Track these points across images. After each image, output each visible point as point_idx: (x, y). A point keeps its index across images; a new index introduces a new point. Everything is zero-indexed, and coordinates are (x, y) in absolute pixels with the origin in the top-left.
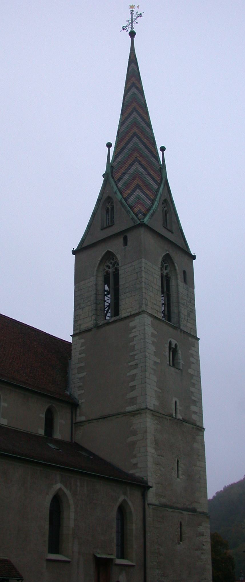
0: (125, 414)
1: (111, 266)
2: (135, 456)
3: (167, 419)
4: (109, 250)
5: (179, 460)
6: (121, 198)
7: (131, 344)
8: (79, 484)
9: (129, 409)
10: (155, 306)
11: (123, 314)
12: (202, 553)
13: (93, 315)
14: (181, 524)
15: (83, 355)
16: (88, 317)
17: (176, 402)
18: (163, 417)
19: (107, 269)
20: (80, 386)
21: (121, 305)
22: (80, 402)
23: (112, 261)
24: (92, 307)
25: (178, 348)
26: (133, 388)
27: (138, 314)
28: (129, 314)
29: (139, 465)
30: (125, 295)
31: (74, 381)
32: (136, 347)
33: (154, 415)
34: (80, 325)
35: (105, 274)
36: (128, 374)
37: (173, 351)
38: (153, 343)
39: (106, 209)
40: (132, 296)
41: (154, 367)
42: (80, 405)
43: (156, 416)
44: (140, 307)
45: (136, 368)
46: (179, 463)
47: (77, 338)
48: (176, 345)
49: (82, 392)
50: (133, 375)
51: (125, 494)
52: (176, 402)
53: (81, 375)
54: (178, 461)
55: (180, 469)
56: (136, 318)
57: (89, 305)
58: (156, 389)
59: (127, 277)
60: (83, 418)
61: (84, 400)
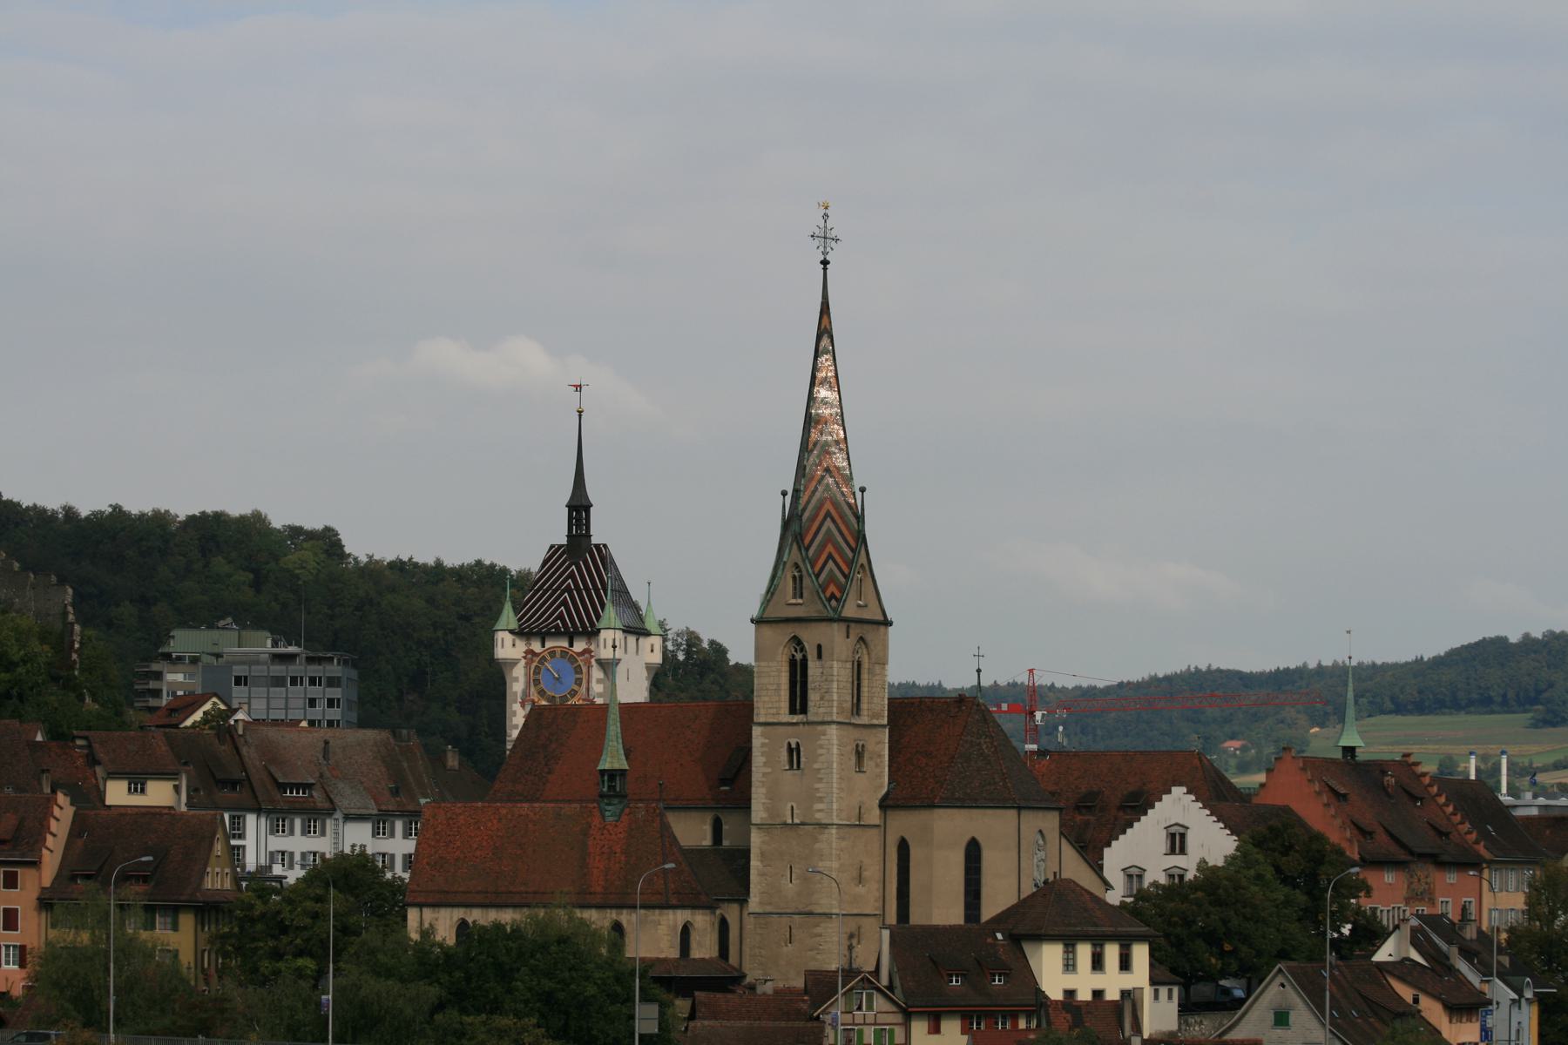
14: (790, 927)
17: (792, 807)
37: (794, 752)
41: (764, 779)
48: (798, 744)
52: (792, 807)
54: (791, 867)
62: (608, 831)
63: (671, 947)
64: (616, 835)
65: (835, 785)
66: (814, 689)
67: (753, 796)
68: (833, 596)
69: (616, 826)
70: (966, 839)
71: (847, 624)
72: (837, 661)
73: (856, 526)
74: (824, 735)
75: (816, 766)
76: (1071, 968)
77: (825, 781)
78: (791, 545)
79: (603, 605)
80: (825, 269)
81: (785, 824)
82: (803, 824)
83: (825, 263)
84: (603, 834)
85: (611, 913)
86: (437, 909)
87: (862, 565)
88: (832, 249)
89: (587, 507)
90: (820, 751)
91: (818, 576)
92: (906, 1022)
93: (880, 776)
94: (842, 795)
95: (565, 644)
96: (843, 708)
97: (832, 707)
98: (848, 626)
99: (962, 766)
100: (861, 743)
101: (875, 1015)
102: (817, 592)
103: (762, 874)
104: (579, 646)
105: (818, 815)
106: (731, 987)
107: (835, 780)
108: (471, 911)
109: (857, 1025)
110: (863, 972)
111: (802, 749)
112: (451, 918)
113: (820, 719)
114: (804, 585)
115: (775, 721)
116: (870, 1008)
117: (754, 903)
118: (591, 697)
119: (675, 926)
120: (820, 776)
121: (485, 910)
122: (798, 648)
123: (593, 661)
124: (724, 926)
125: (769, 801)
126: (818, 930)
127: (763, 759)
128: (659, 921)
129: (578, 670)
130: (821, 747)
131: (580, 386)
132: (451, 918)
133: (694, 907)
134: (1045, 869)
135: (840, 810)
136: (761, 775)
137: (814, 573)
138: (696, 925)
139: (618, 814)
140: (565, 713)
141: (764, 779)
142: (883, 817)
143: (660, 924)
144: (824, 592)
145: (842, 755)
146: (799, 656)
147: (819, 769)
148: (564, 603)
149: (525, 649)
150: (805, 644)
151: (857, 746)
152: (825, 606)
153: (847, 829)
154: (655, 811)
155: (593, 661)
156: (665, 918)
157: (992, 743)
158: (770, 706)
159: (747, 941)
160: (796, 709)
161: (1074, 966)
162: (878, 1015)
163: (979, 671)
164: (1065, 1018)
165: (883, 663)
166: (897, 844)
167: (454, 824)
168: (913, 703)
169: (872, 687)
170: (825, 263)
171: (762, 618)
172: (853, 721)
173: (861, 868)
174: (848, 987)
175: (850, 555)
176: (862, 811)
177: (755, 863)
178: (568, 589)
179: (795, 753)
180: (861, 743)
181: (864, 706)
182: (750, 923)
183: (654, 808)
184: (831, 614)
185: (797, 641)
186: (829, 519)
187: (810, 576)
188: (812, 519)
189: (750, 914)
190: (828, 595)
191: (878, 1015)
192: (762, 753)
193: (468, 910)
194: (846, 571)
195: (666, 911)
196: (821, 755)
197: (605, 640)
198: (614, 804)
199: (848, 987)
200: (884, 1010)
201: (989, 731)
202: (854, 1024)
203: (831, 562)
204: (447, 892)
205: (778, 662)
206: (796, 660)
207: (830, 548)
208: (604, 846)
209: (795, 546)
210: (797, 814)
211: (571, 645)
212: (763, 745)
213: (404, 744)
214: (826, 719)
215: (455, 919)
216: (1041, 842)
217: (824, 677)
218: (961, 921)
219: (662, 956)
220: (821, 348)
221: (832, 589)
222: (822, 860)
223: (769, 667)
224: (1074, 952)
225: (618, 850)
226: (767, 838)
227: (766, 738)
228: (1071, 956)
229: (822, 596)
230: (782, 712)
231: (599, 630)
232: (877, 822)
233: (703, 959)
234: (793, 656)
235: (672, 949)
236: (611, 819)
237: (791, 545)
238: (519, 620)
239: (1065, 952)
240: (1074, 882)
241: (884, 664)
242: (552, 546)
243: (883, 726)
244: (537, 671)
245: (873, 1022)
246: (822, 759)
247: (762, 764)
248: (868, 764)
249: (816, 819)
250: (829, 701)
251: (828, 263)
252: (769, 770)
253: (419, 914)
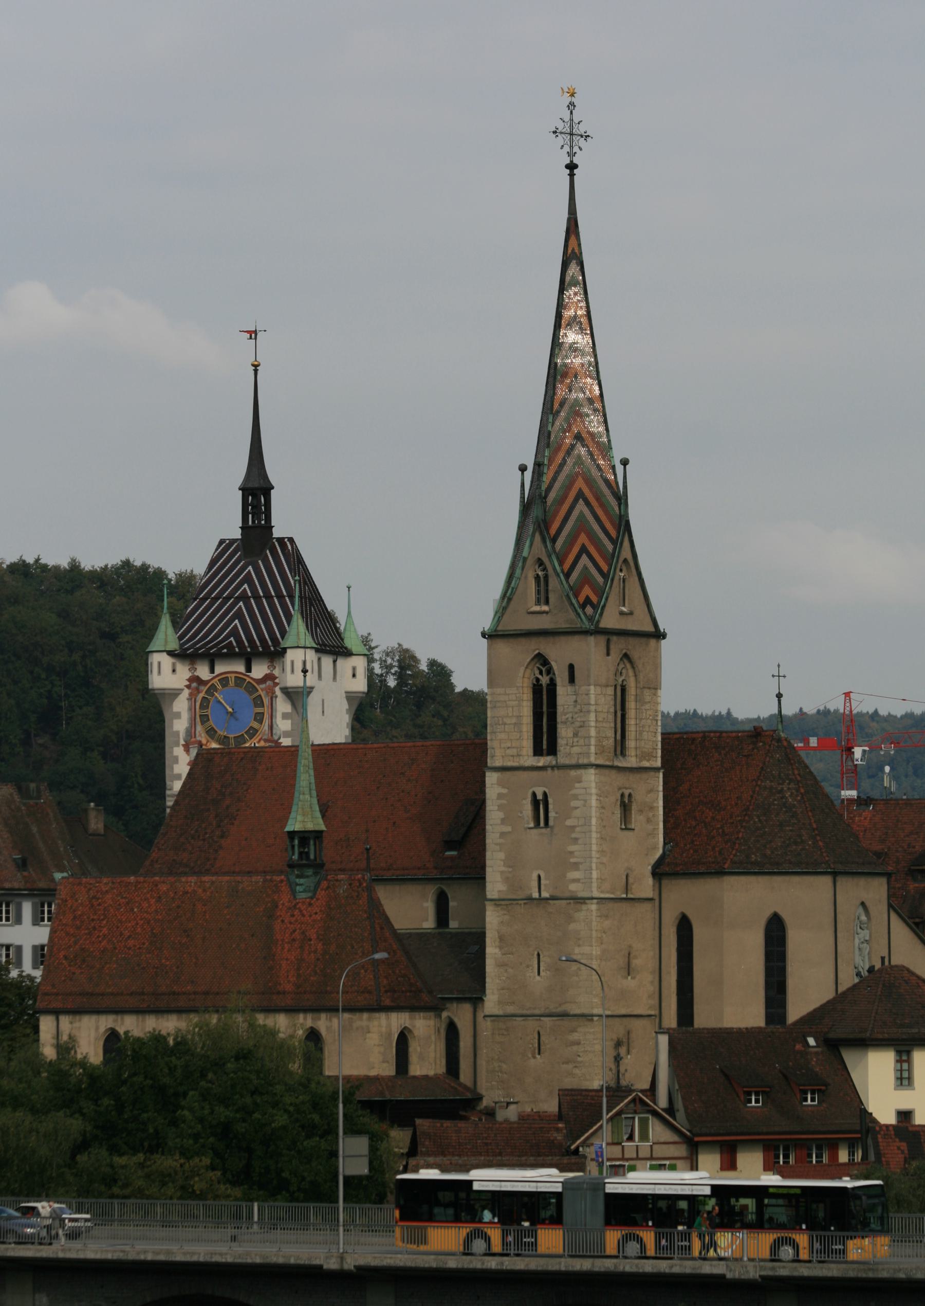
3: (521, 904)
5: (540, 953)
12: (576, 1067)
17: (539, 877)
18: (512, 904)
37: (540, 805)
38: (500, 808)
41: (501, 841)
43: (501, 905)
46: (541, 957)
48: (545, 794)
52: (539, 877)
54: (539, 955)
55: (542, 964)
58: (503, 869)
62: (301, 911)
63: (383, 1062)
64: (310, 916)
65: (594, 847)
66: (565, 723)
67: (488, 863)
68: (588, 601)
69: (310, 904)
70: (767, 914)
71: (607, 637)
72: (595, 685)
73: (617, 509)
74: (580, 782)
75: (569, 823)
76: (905, 1082)
77: (580, 842)
78: (533, 536)
79: (289, 617)
80: (572, 175)
81: (530, 899)
82: (553, 898)
83: (572, 167)
84: (293, 916)
85: (305, 1019)
86: (78, 1017)
87: (625, 561)
88: (580, 149)
89: (267, 489)
90: (574, 803)
91: (568, 575)
92: (692, 1154)
93: (653, 834)
94: (605, 860)
95: (241, 668)
96: (603, 747)
97: (589, 745)
98: (608, 641)
99: (760, 820)
100: (627, 792)
101: (651, 1146)
102: (568, 596)
103: (501, 965)
104: (259, 670)
105: (573, 887)
106: (462, 1113)
107: (594, 841)
108: (122, 1019)
109: (627, 1160)
110: (634, 1091)
111: (550, 800)
112: (97, 1028)
113: (574, 762)
114: (550, 588)
115: (515, 764)
116: (644, 1137)
117: (492, 1002)
118: (276, 738)
119: (390, 1034)
120: (573, 835)
121: (140, 1017)
122: (544, 669)
123: (277, 689)
124: (452, 1032)
125: (510, 870)
126: (575, 1036)
127: (501, 815)
128: (368, 1027)
129: (258, 702)
130: (576, 797)
131: (255, 332)
132: (97, 1028)
133: (413, 1008)
134: (869, 953)
135: (601, 880)
136: (498, 835)
137: (563, 571)
138: (416, 1033)
139: (312, 888)
140: (242, 759)
141: (501, 841)
142: (657, 885)
143: (369, 1032)
144: (576, 596)
145: (603, 808)
146: (544, 680)
147: (574, 827)
148: (239, 615)
149: (188, 675)
150: (553, 664)
151: (622, 795)
152: (578, 614)
153: (611, 905)
154: (361, 884)
155: (277, 689)
156: (376, 1023)
157: (798, 790)
158: (509, 745)
159: (483, 1052)
160: (542, 749)
161: (910, 1079)
162: (655, 1147)
163: (779, 696)
164: (899, 1148)
165: (654, 686)
166: (677, 922)
167: (99, 905)
168: (694, 739)
169: (641, 719)
170: (572, 167)
171: (496, 631)
172: (617, 763)
173: (629, 954)
174: (614, 1111)
175: (610, 547)
176: (631, 880)
177: (492, 950)
178: (244, 597)
179: (541, 806)
180: (627, 792)
181: (631, 744)
182: (486, 1027)
183: (359, 880)
184: (587, 625)
185: (542, 661)
186: (581, 501)
187: (558, 575)
188: (561, 501)
189: (485, 1016)
190: (582, 599)
191: (655, 1147)
192: (498, 806)
193: (119, 1017)
194: (605, 568)
195: (377, 1015)
196: (576, 808)
197: (292, 662)
198: (307, 877)
199: (614, 1111)
200: (662, 1140)
201: (794, 774)
202: (623, 1159)
203: (584, 557)
204: (92, 994)
205: (518, 687)
206: (541, 685)
207: (583, 539)
208: (294, 931)
209: (538, 537)
210: (545, 885)
211: (249, 669)
212: (500, 796)
213: (32, 802)
214: (581, 762)
215: (102, 1029)
216: (864, 918)
217: (578, 707)
218: (760, 1022)
219: (373, 1073)
220: (568, 279)
221: (587, 591)
222: (579, 946)
223: (505, 694)
224: (909, 1061)
225: (314, 936)
226: (507, 917)
227: (503, 787)
228: (905, 1066)
229: (574, 601)
230: (524, 752)
231: (284, 650)
232: (650, 894)
233: (426, 1077)
234: (538, 680)
235: (385, 1065)
236: (303, 895)
237: (533, 536)
238: (180, 638)
239: (897, 1061)
240: (908, 970)
241: (656, 689)
242: (222, 542)
243: (656, 770)
244: (205, 703)
245: (649, 1156)
246: (577, 813)
247: (499, 822)
248: (637, 819)
249: (570, 891)
250: (585, 737)
251: (576, 166)
252: (509, 829)
253: (55, 1023)
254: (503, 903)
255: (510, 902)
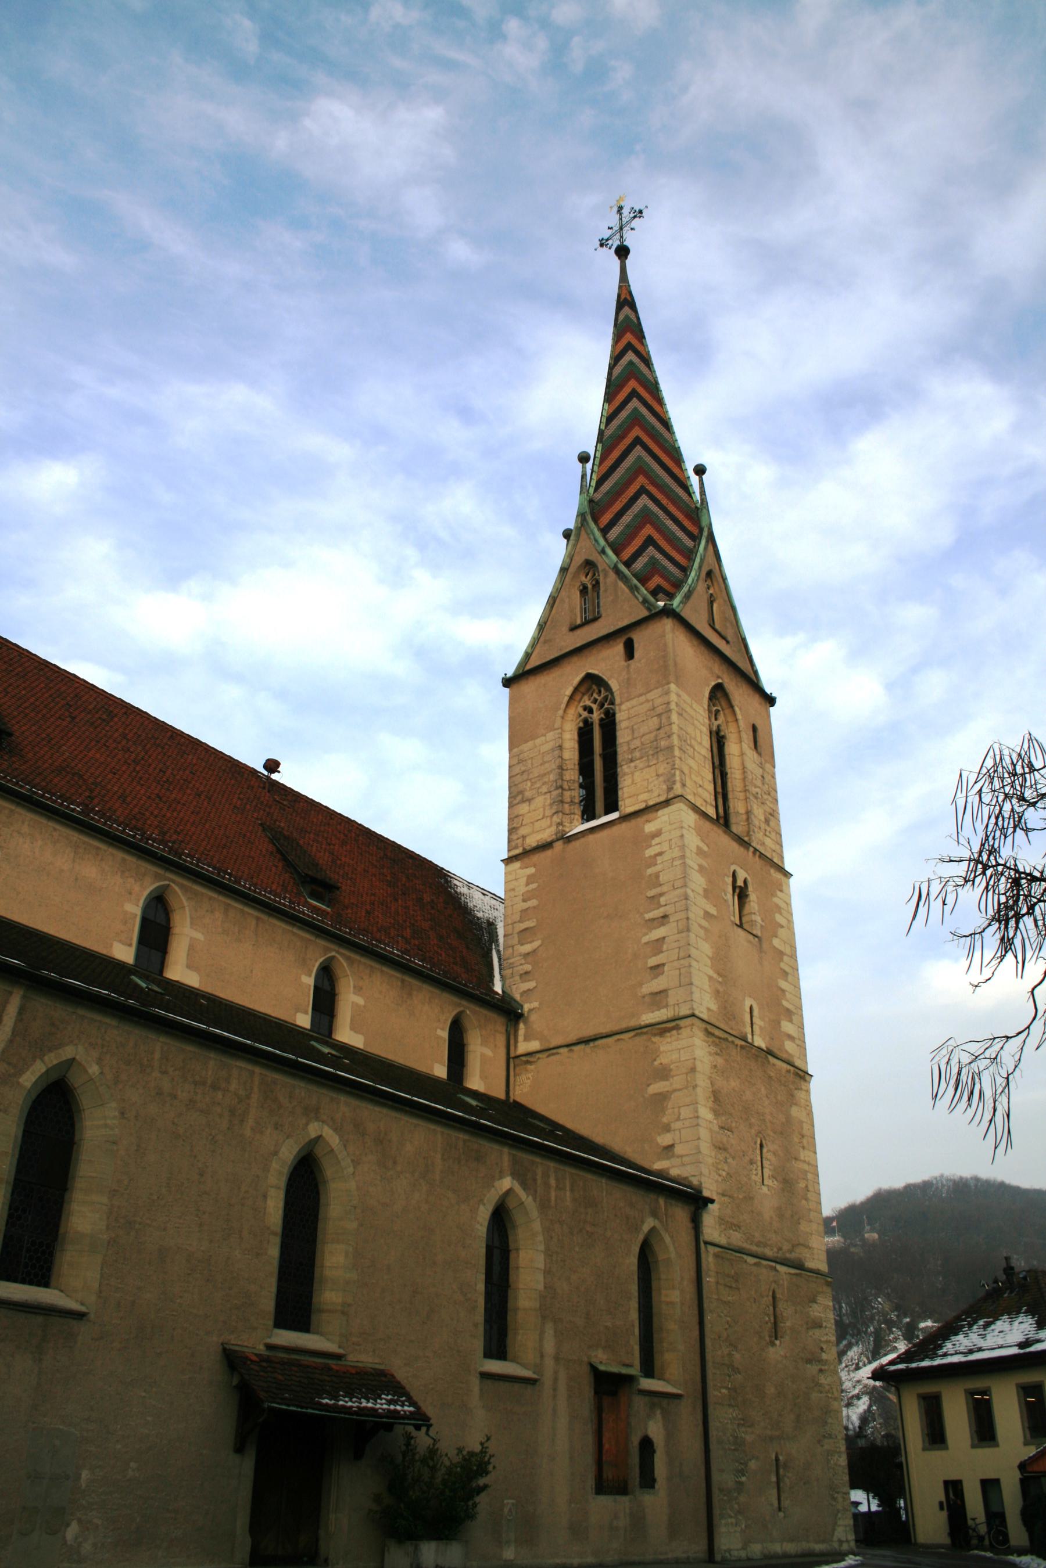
0: (638, 1030)
1: (595, 707)
2: (667, 1129)
3: (737, 1045)
4: (590, 671)
5: (764, 1142)
6: (615, 561)
7: (649, 871)
8: (553, 1182)
9: (649, 1017)
10: (700, 789)
11: (628, 804)
12: (821, 1370)
13: (555, 813)
14: (774, 1298)
15: (533, 903)
16: (543, 818)
17: (751, 1008)
19: (585, 714)
20: (526, 973)
21: (622, 788)
22: (526, 1007)
23: (597, 697)
24: (552, 797)
25: (750, 888)
26: (657, 969)
27: (667, 803)
28: (643, 806)
29: (679, 1150)
30: (632, 764)
31: (511, 961)
32: (663, 878)
33: (709, 1034)
34: (524, 837)
35: (581, 725)
36: (645, 939)
38: (701, 869)
39: (581, 588)
40: (649, 766)
42: (526, 1015)
43: (713, 1035)
44: (670, 789)
45: (663, 924)
46: (765, 1150)
47: (517, 865)
49: (531, 985)
50: (657, 940)
51: (654, 1214)
52: (751, 1008)
53: (527, 948)
54: (761, 1146)
56: (660, 813)
57: (546, 793)
58: (711, 973)
59: (635, 727)
60: (534, 1045)
61: (536, 1004)
254: (717, 1032)
255: (725, 1036)
